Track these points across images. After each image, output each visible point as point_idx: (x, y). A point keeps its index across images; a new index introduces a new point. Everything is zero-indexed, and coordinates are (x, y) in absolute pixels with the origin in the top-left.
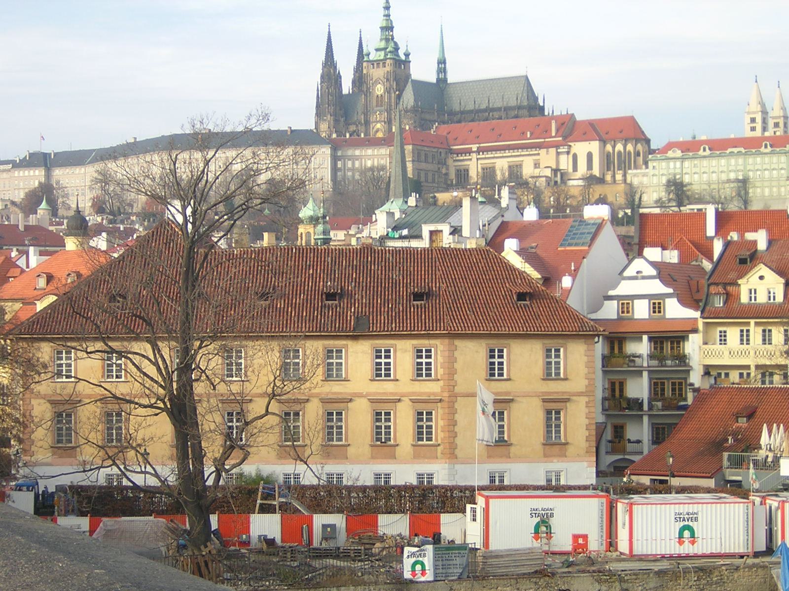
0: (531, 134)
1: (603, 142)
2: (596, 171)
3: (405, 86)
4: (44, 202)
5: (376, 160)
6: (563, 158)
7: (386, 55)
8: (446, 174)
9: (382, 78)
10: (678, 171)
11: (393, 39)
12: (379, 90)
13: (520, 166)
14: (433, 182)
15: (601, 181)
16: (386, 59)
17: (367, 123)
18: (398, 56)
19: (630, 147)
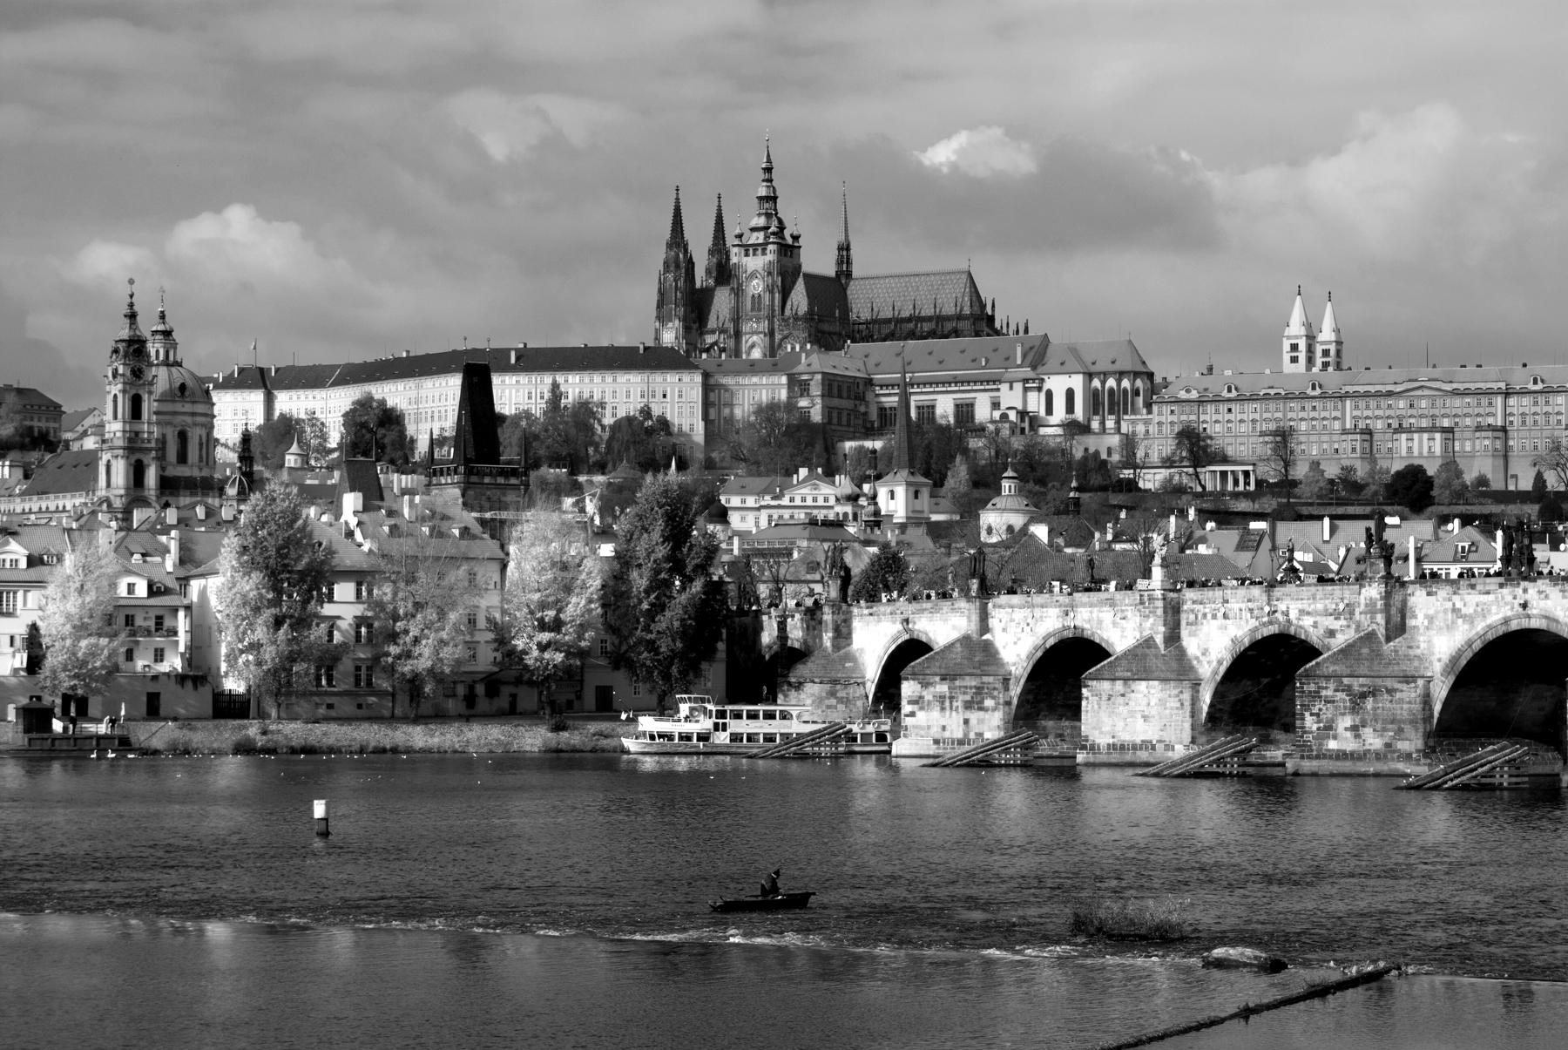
0: (987, 361)
1: (1090, 376)
2: (1079, 413)
3: (794, 283)
4: (295, 445)
5: (764, 392)
6: (1033, 396)
7: (766, 237)
8: (866, 414)
9: (760, 270)
10: (1193, 417)
11: (776, 214)
12: (756, 287)
13: (972, 405)
14: (849, 425)
15: (1085, 429)
16: (768, 244)
17: (738, 335)
18: (783, 238)
19: (1126, 383)
